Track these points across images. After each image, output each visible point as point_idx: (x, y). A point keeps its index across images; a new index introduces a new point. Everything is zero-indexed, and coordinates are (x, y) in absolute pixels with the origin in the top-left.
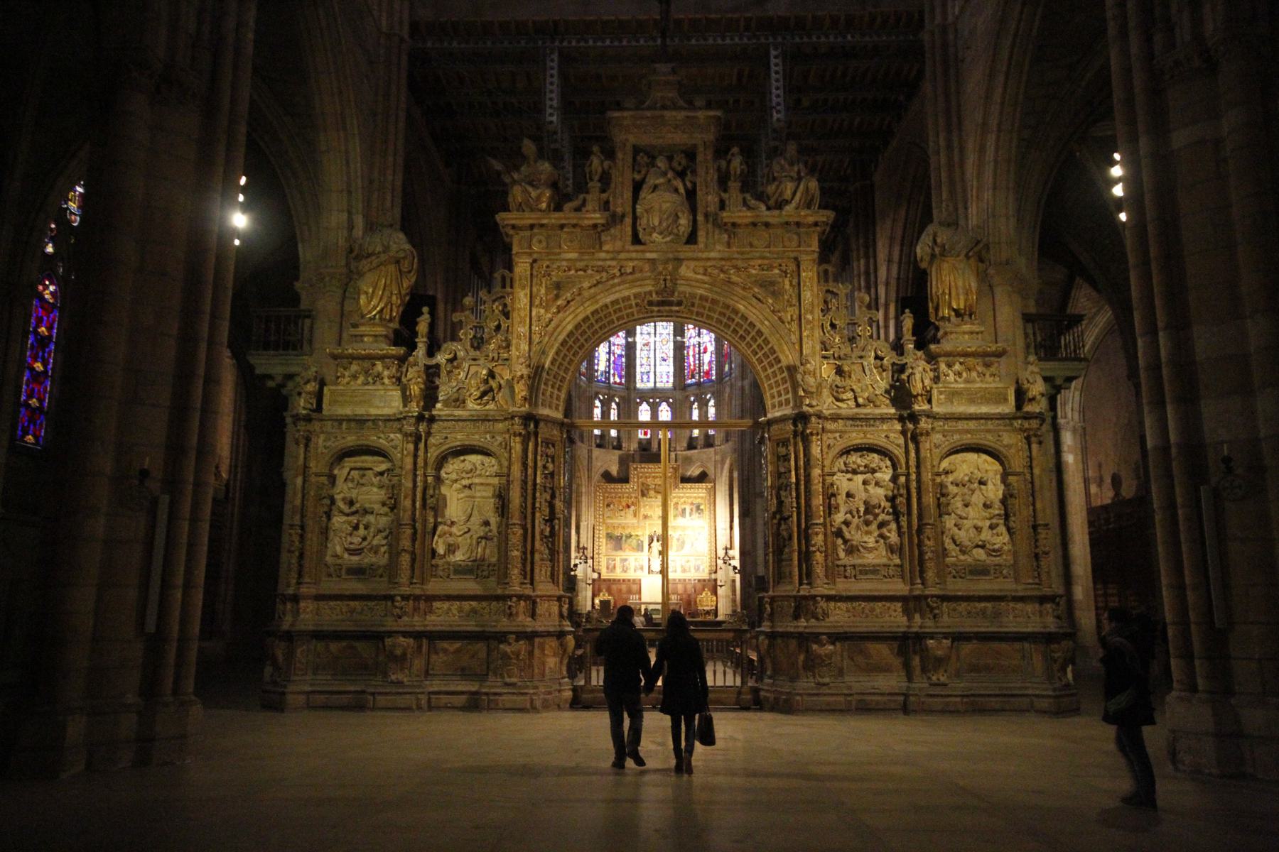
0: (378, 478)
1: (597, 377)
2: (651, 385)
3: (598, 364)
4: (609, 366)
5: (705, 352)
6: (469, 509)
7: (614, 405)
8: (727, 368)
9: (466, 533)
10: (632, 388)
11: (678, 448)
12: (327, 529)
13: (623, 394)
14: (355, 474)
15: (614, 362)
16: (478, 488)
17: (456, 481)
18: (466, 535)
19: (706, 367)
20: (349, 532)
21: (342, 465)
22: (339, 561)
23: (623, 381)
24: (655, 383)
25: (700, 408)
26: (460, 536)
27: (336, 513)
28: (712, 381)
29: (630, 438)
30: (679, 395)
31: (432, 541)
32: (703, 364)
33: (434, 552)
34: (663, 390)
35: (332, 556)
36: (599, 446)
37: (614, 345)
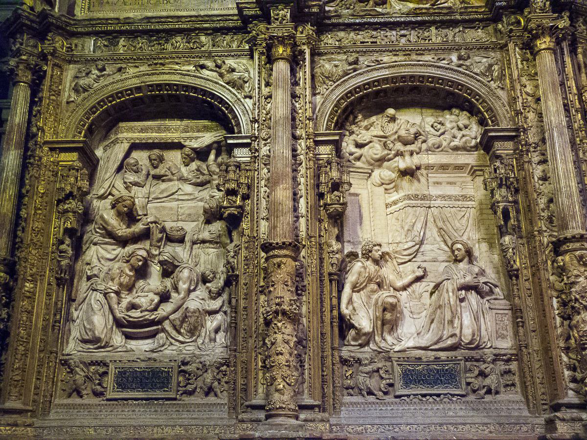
0: (194, 165)
6: (419, 226)
9: (418, 279)
12: (71, 270)
14: (141, 157)
16: (434, 177)
17: (381, 161)
18: (418, 287)
20: (125, 280)
21: (113, 137)
22: (100, 355)
26: (404, 288)
27: (97, 238)
31: (339, 298)
33: (344, 325)
35: (85, 341)
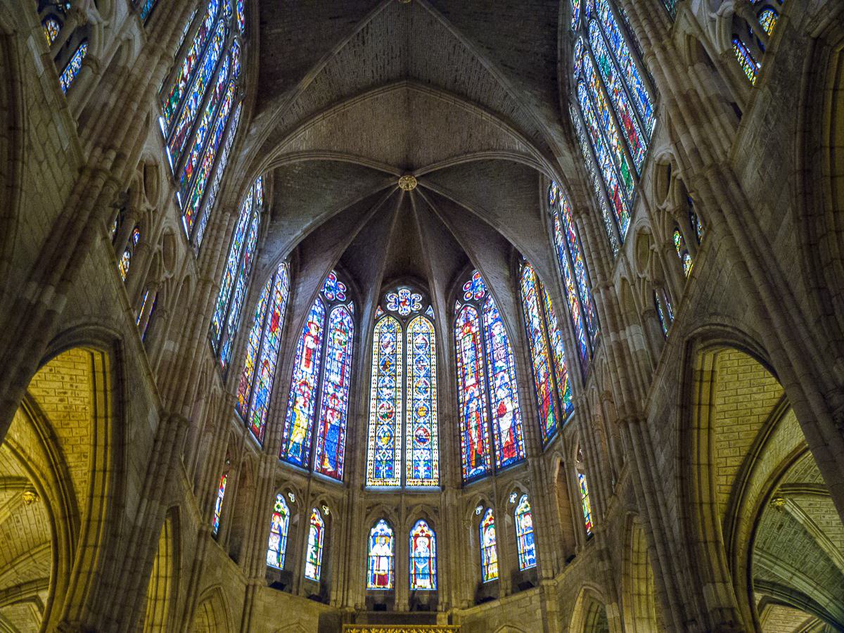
1: (286, 452)
2: (394, 483)
3: (290, 431)
4: (313, 440)
5: (501, 416)
7: (317, 519)
8: (550, 421)
10: (358, 483)
11: (454, 603)
13: (340, 494)
15: (324, 435)
19: (506, 439)
23: (340, 470)
24: (403, 478)
25: (498, 516)
28: (523, 459)
29: (347, 579)
30: (451, 498)
32: (500, 434)
34: (415, 493)
36: (278, 586)
37: (328, 408)
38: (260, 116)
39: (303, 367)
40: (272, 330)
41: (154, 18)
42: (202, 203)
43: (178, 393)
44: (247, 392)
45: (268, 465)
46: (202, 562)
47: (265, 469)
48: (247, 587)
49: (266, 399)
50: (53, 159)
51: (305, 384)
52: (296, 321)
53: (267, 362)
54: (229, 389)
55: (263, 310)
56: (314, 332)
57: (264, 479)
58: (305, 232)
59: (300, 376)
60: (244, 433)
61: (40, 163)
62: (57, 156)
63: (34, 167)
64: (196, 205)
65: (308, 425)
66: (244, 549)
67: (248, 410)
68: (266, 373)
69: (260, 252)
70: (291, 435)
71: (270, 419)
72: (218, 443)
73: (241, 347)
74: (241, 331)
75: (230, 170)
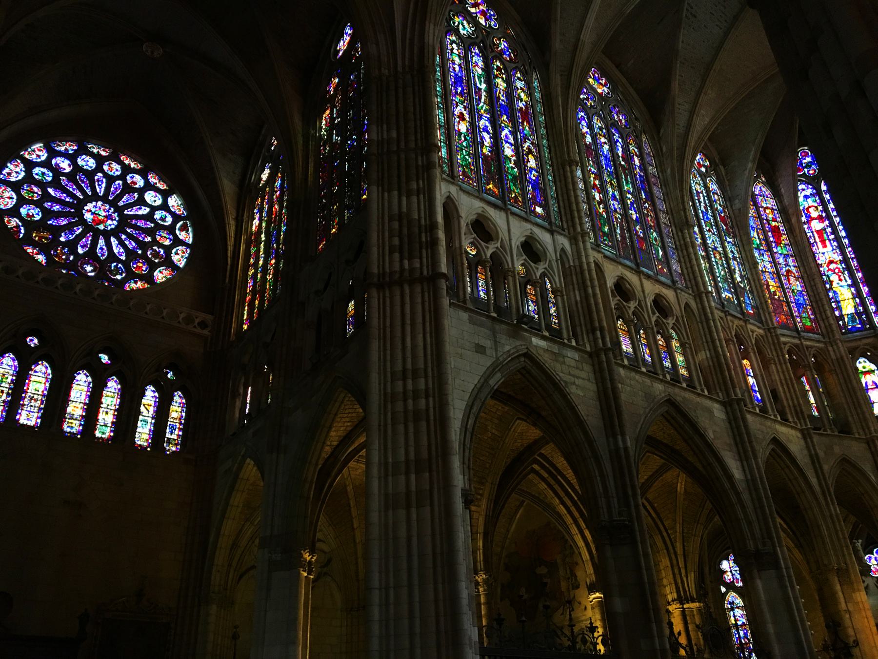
3: (839, 308)
4: (863, 303)
38: (662, 131)
39: (821, 250)
40: (778, 243)
41: (563, 213)
42: (664, 249)
43: (725, 382)
44: (786, 308)
45: (835, 347)
46: (817, 454)
47: (834, 351)
48: (868, 443)
49: (804, 299)
50: (577, 372)
51: (831, 262)
52: (794, 220)
53: (788, 271)
54: (768, 325)
55: (761, 237)
56: (814, 214)
57: (837, 359)
58: (754, 162)
59: (823, 259)
60: (800, 340)
61: (574, 383)
62: (577, 368)
63: (573, 389)
64: (661, 253)
65: (852, 294)
66: (850, 419)
67: (794, 321)
68: (792, 279)
69: (730, 201)
70: (841, 311)
71: (818, 312)
72: (782, 368)
73: (758, 287)
74: (752, 274)
75: (668, 196)
